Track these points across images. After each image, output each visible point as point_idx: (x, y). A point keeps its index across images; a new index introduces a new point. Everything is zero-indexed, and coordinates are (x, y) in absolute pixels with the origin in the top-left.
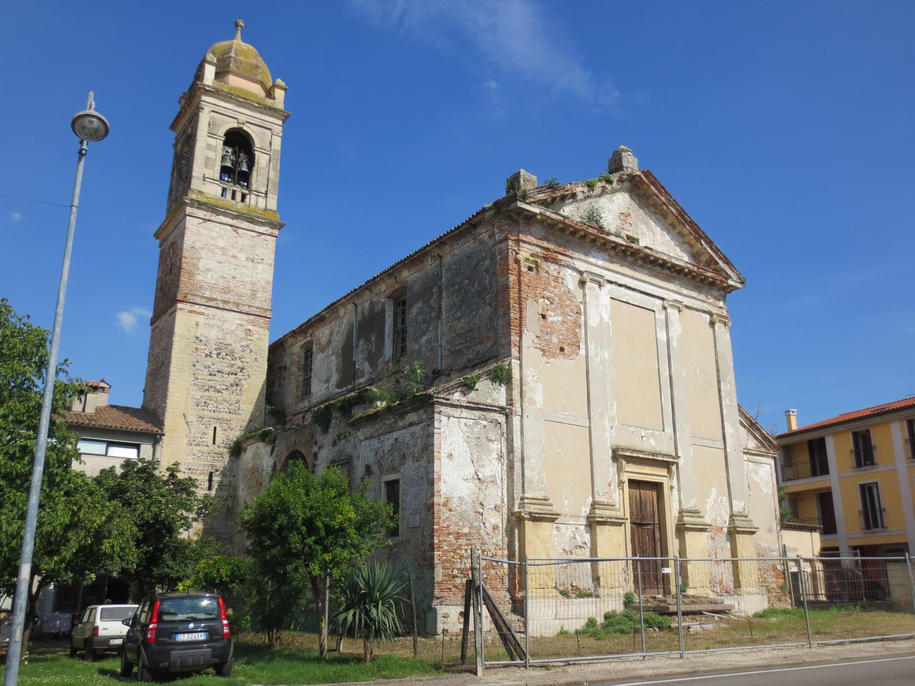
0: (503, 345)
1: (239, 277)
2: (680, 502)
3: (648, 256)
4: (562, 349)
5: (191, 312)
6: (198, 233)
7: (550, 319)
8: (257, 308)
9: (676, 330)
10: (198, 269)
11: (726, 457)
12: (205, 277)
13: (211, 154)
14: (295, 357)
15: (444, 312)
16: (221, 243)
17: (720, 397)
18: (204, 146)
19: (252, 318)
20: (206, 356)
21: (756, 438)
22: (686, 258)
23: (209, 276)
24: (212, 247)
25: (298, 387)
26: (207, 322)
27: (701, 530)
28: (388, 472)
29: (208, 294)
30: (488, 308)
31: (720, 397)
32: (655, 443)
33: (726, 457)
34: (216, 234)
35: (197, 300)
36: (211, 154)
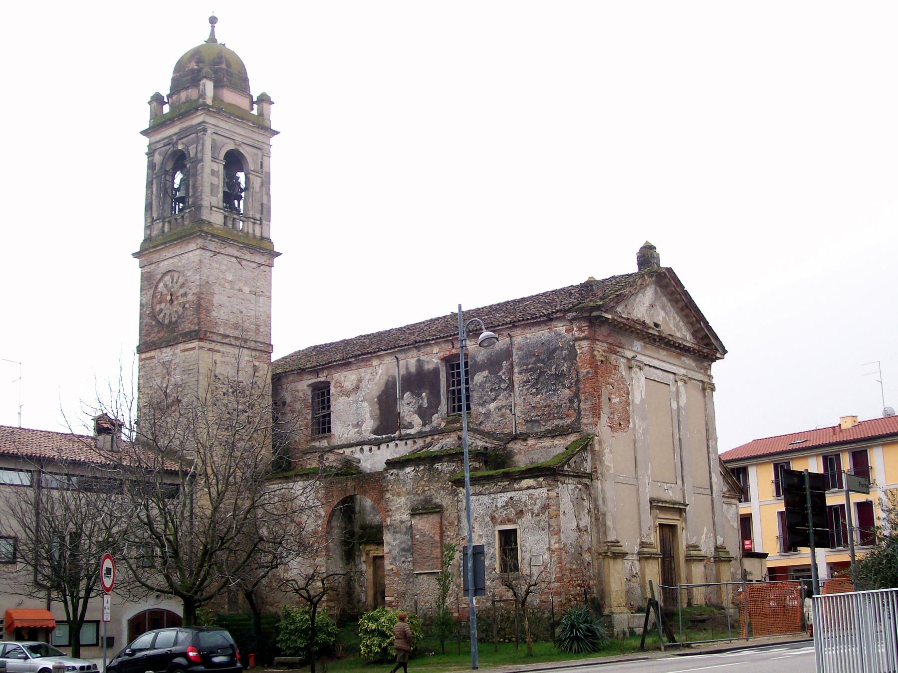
0: (586, 424)
1: (244, 310)
2: (687, 539)
3: (669, 341)
4: (620, 424)
5: (210, 350)
6: (211, 267)
7: (613, 401)
8: (262, 343)
9: (683, 400)
10: (213, 305)
11: (712, 501)
12: (219, 313)
13: (215, 180)
14: (301, 394)
15: (516, 386)
16: (230, 277)
17: (708, 452)
18: (209, 172)
19: (257, 353)
20: (224, 394)
21: (728, 483)
22: (689, 337)
23: (222, 312)
24: (223, 281)
25: (307, 426)
26: (223, 359)
27: (701, 560)
28: (502, 523)
29: (222, 331)
30: (567, 391)
31: (708, 452)
32: (672, 494)
33: (712, 501)
34: (225, 268)
35: (215, 338)
36: (215, 180)
